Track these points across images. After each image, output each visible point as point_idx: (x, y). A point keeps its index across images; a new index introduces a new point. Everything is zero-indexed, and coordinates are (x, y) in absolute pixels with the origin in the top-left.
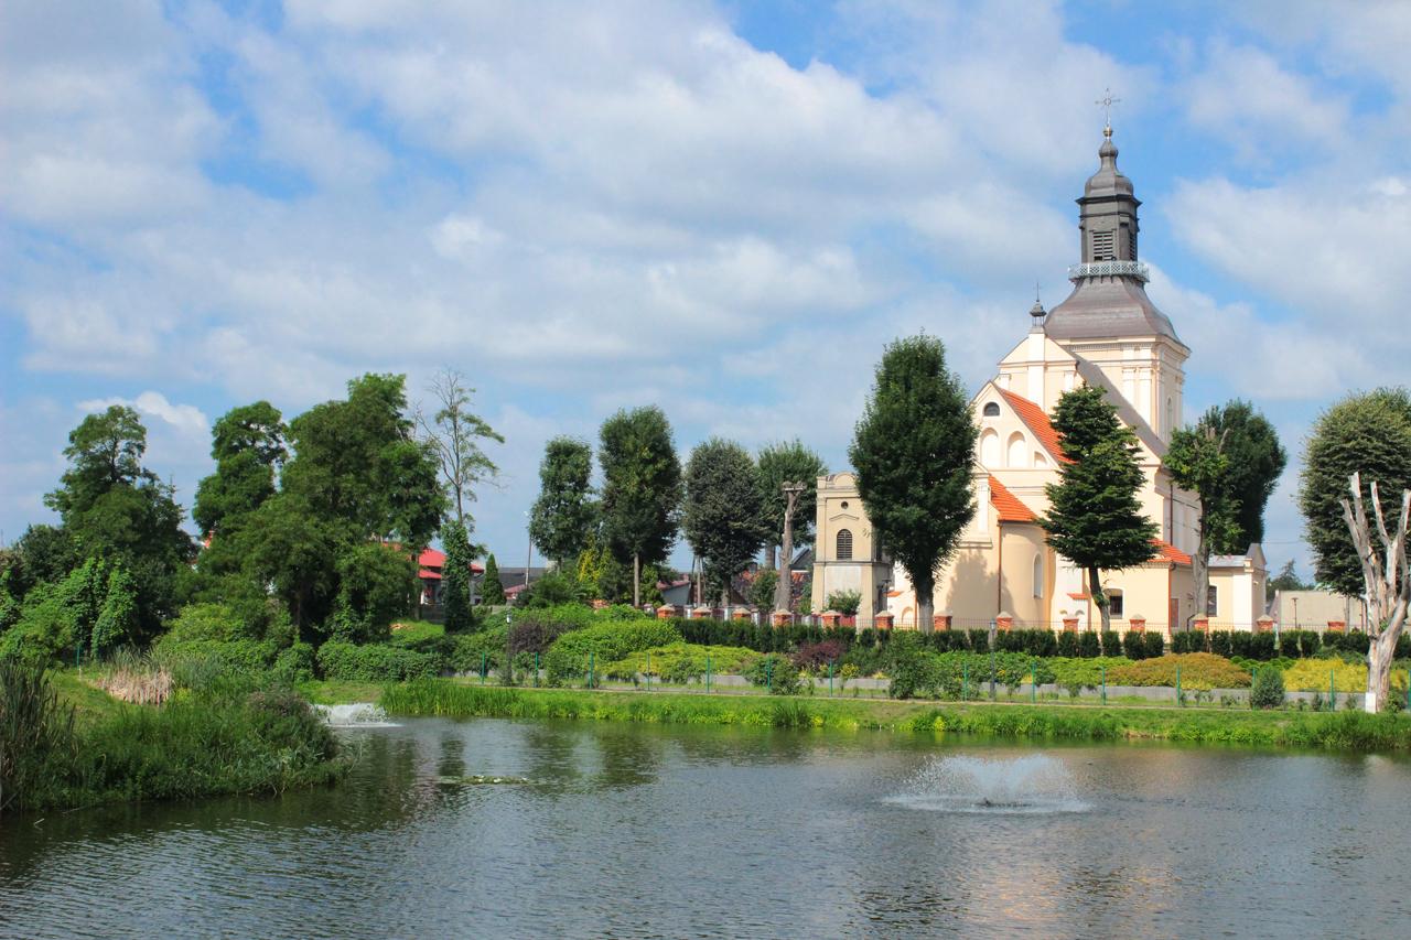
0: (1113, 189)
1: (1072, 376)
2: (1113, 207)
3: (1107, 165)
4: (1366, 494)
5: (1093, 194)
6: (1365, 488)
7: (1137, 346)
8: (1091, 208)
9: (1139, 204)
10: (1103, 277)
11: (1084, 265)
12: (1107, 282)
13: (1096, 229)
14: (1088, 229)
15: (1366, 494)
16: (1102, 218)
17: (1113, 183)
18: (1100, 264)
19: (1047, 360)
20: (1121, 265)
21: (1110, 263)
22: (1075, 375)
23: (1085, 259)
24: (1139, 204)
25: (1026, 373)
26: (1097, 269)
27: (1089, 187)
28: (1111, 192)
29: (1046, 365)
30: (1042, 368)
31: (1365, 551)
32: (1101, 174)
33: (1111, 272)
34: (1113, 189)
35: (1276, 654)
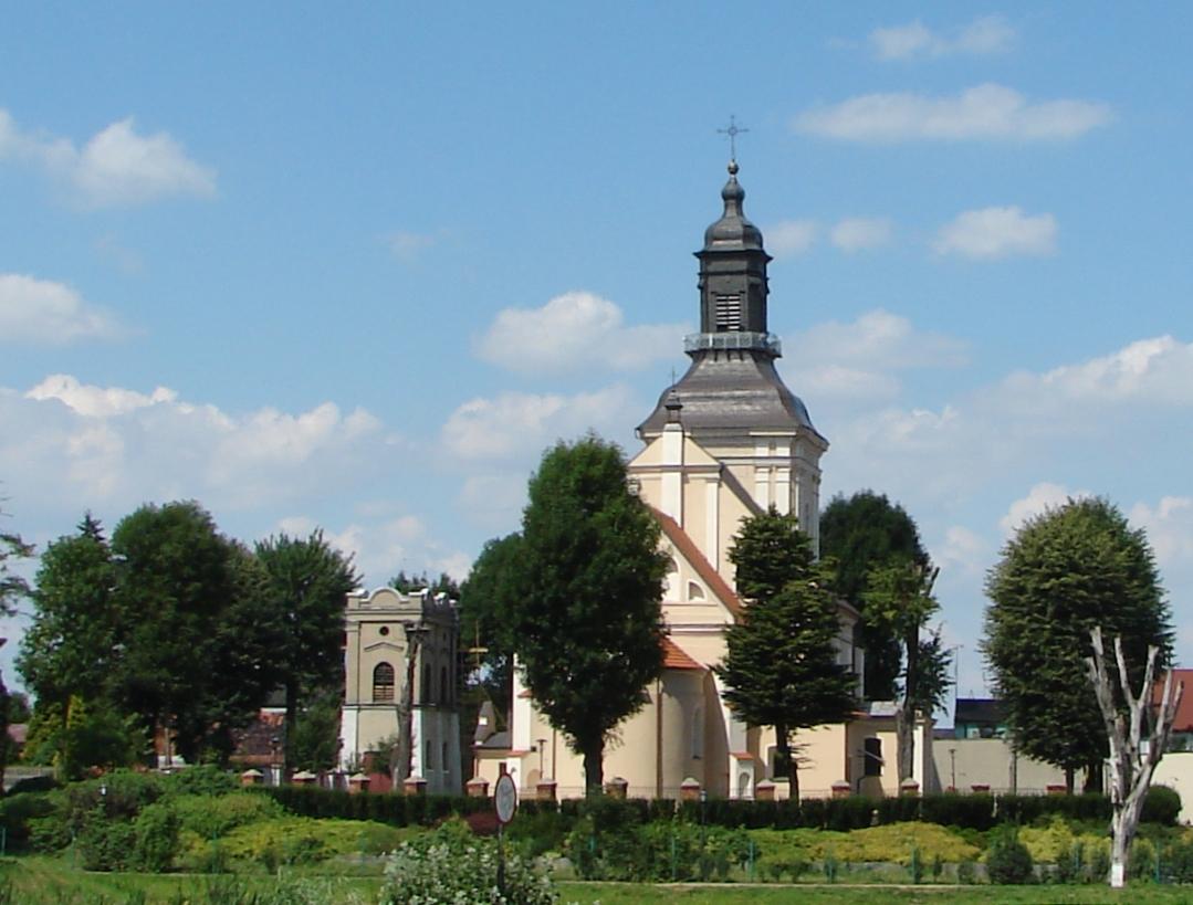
0: (740, 242)
1: (715, 485)
2: (743, 265)
3: (732, 212)
4: (1109, 654)
5: (720, 245)
6: (1105, 642)
7: (772, 443)
8: (715, 266)
9: (770, 259)
10: (729, 350)
11: (705, 335)
12: (723, 360)
13: (720, 290)
14: (710, 290)
15: (1109, 654)
16: (727, 278)
17: (741, 233)
18: (724, 336)
19: (686, 464)
20: (745, 338)
21: (738, 335)
22: (720, 486)
23: (705, 328)
24: (770, 259)
25: (660, 479)
26: (721, 341)
27: (711, 236)
28: (738, 245)
29: (685, 471)
30: (678, 475)
31: (1110, 714)
32: (726, 221)
33: (738, 345)
34: (740, 242)
35: (993, 822)
